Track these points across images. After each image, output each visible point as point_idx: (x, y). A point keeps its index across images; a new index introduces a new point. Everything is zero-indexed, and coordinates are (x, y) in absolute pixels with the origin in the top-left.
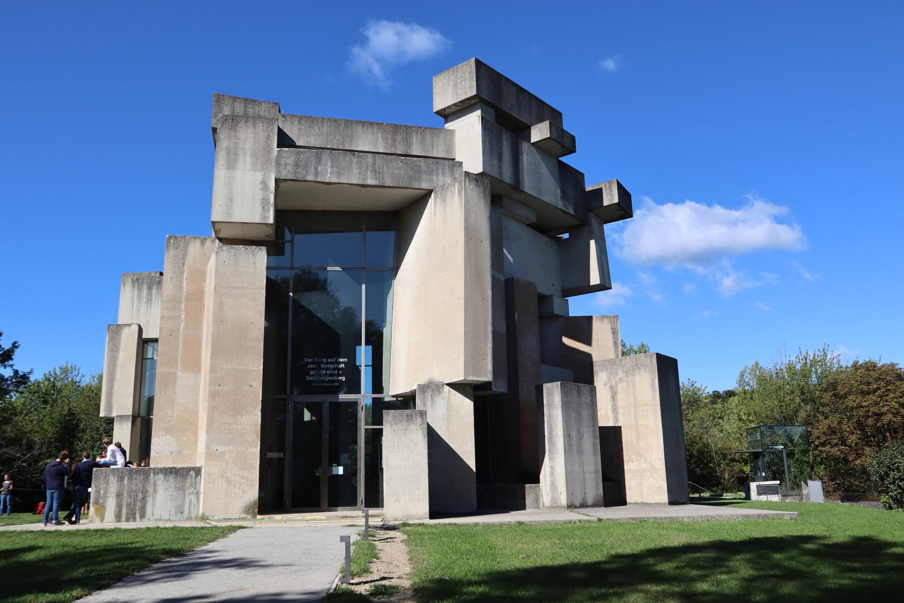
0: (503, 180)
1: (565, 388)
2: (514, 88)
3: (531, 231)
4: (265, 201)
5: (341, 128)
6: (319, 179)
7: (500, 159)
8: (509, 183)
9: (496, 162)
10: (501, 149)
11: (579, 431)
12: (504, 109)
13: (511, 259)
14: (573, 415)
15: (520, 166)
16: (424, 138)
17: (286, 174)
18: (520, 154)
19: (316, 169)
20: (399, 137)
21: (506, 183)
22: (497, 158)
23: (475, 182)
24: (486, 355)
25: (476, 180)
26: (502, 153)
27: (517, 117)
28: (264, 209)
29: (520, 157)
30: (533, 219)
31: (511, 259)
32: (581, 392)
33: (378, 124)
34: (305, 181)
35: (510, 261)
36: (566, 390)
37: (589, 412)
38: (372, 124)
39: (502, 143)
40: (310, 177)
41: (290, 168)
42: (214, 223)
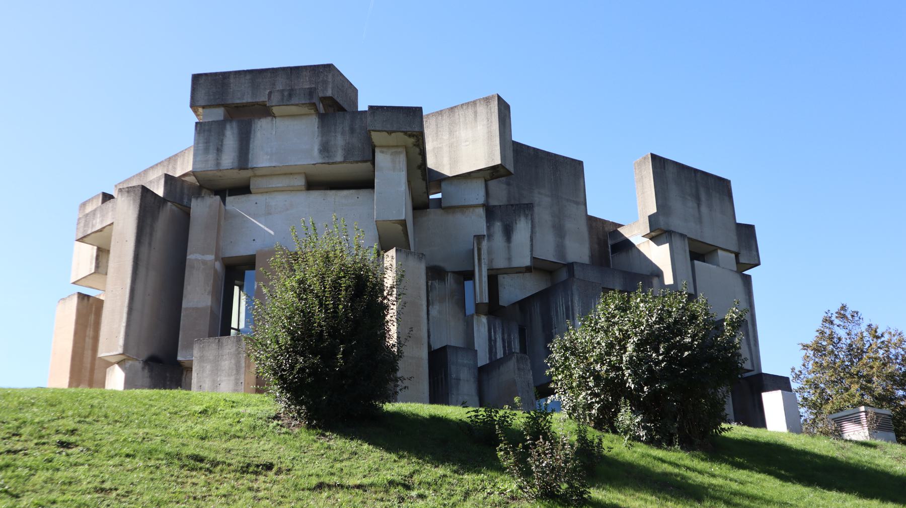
0: (221, 168)
1: (201, 344)
2: (248, 77)
3: (316, 196)
4: (92, 256)
5: (142, 178)
6: (93, 231)
7: (219, 150)
8: (229, 168)
9: (212, 157)
10: (222, 141)
11: (214, 381)
12: (230, 102)
13: (272, 233)
14: (208, 367)
15: (251, 146)
16: (184, 158)
17: (81, 236)
18: (253, 132)
19: (92, 223)
20: (170, 167)
21: (227, 169)
22: (215, 151)
23: (126, 194)
24: (119, 333)
25: (128, 192)
26: (222, 145)
27: (250, 100)
28: (91, 263)
29: (252, 136)
30: (300, 182)
31: (272, 233)
32: (222, 343)
33: (160, 163)
34: (89, 235)
35: (270, 234)
36: (202, 346)
37: (233, 361)
38: (157, 165)
39: (223, 135)
40: (89, 232)
41: (81, 230)
42: (74, 283)
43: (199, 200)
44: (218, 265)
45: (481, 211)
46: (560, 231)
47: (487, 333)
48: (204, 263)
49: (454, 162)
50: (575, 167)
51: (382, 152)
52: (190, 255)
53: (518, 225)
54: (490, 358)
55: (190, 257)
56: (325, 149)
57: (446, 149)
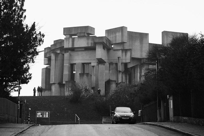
7: (69, 44)
43: (66, 53)
44: (70, 66)
45: (121, 51)
46: (141, 51)
47: (121, 76)
48: (67, 66)
49: (115, 40)
50: (147, 35)
51: (98, 45)
52: (65, 64)
53: (128, 54)
54: (122, 81)
55: (64, 64)
56: (88, 44)
57: (114, 37)
